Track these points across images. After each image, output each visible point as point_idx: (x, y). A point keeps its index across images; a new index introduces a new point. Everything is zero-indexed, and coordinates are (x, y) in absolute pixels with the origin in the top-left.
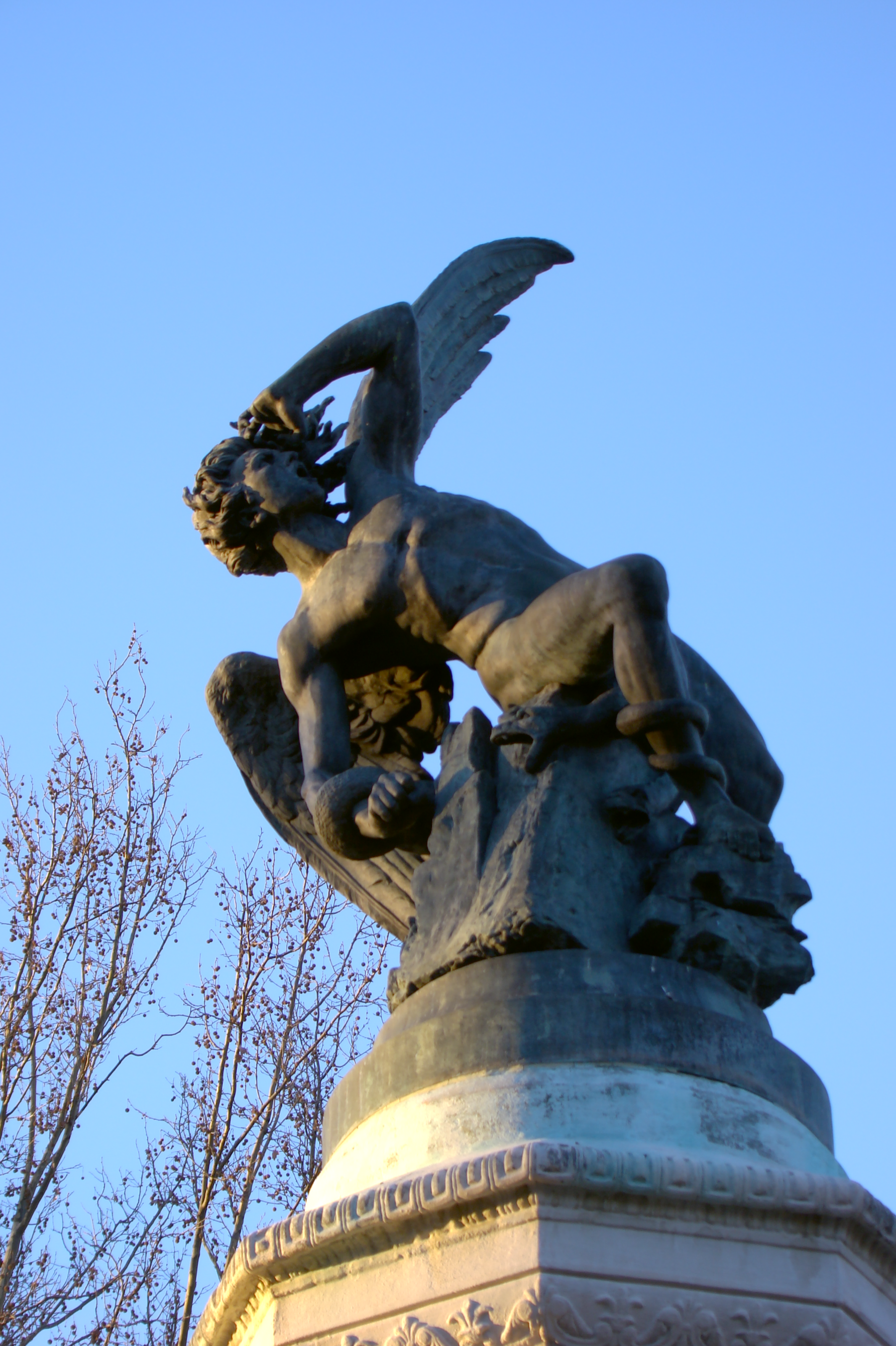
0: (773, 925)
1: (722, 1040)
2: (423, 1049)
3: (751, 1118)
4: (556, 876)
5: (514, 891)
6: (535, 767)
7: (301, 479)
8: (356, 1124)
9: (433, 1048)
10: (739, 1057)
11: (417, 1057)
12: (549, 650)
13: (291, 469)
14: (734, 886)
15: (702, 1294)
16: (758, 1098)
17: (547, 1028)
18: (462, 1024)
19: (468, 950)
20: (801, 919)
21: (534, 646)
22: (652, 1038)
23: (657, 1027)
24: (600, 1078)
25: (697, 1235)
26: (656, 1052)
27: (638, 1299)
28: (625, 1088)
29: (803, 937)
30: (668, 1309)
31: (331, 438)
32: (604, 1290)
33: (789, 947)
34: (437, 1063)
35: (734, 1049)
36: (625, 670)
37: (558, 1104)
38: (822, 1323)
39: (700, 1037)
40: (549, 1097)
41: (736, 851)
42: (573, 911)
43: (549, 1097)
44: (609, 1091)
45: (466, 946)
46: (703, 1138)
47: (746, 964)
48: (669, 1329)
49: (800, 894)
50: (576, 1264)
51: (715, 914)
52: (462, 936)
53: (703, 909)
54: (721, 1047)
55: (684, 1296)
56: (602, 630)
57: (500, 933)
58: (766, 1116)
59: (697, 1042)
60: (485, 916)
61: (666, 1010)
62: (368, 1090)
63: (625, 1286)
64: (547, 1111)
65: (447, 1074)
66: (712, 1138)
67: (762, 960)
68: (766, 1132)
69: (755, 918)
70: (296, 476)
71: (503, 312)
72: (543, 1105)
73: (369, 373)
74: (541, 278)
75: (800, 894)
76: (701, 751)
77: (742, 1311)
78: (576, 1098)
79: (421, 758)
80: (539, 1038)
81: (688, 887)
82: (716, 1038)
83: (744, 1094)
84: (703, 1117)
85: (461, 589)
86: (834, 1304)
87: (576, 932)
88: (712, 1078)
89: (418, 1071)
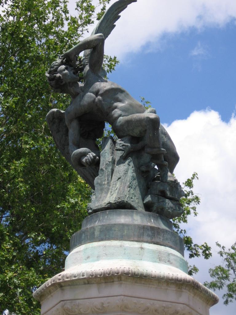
0: (176, 203)
1: (163, 235)
4: (129, 189)
7: (74, 75)
8: (80, 245)
10: (167, 239)
11: (95, 233)
14: (168, 193)
16: (170, 249)
17: (126, 232)
18: (106, 228)
19: (108, 205)
22: (148, 235)
23: (150, 233)
24: (136, 245)
26: (149, 239)
27: (142, 302)
30: (149, 305)
33: (179, 208)
34: (100, 236)
35: (166, 237)
39: (159, 235)
41: (169, 185)
42: (132, 198)
45: (107, 204)
46: (158, 260)
48: (148, 309)
50: (130, 294)
51: (163, 201)
53: (161, 199)
54: (163, 237)
55: (152, 302)
57: (115, 203)
59: (158, 236)
60: (112, 197)
61: (152, 228)
65: (102, 240)
67: (172, 211)
69: (172, 201)
70: (73, 74)
71: (119, 15)
74: (128, 6)
76: (163, 160)
77: (164, 305)
80: (124, 234)
81: (157, 192)
82: (162, 234)
83: (167, 248)
85: (110, 107)
87: (133, 204)
88: (161, 245)
89: (95, 237)
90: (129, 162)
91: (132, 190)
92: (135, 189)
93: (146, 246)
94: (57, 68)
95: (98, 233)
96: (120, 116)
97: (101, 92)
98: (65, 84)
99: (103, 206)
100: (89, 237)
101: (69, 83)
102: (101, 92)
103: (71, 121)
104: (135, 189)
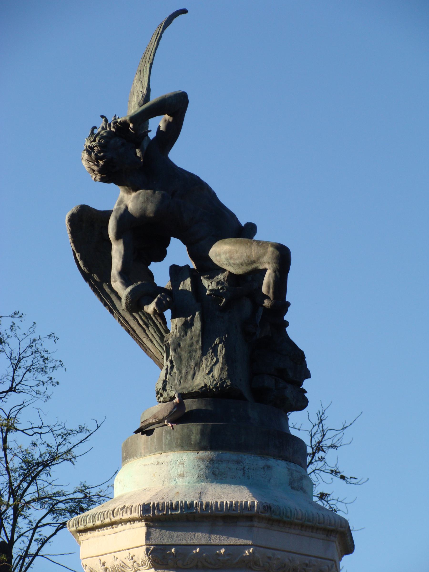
2: (195, 434)
5: (222, 369)
9: (199, 436)
11: (192, 437)
12: (234, 264)
15: (297, 555)
20: (306, 385)
21: (227, 259)
24: (261, 462)
25: (297, 534)
32: (269, 553)
34: (200, 443)
36: (269, 287)
37: (247, 471)
38: (328, 566)
40: (244, 468)
43: (244, 468)
44: (264, 468)
45: (202, 387)
46: (289, 487)
49: (308, 375)
56: (261, 267)
62: (167, 441)
63: (276, 552)
64: (244, 473)
66: (292, 488)
72: (242, 470)
75: (308, 375)
77: (307, 562)
78: (253, 469)
79: (149, 264)
84: (290, 479)
86: (332, 560)
93: (272, 462)
95: (198, 437)
99: (196, 389)
100: (179, 440)
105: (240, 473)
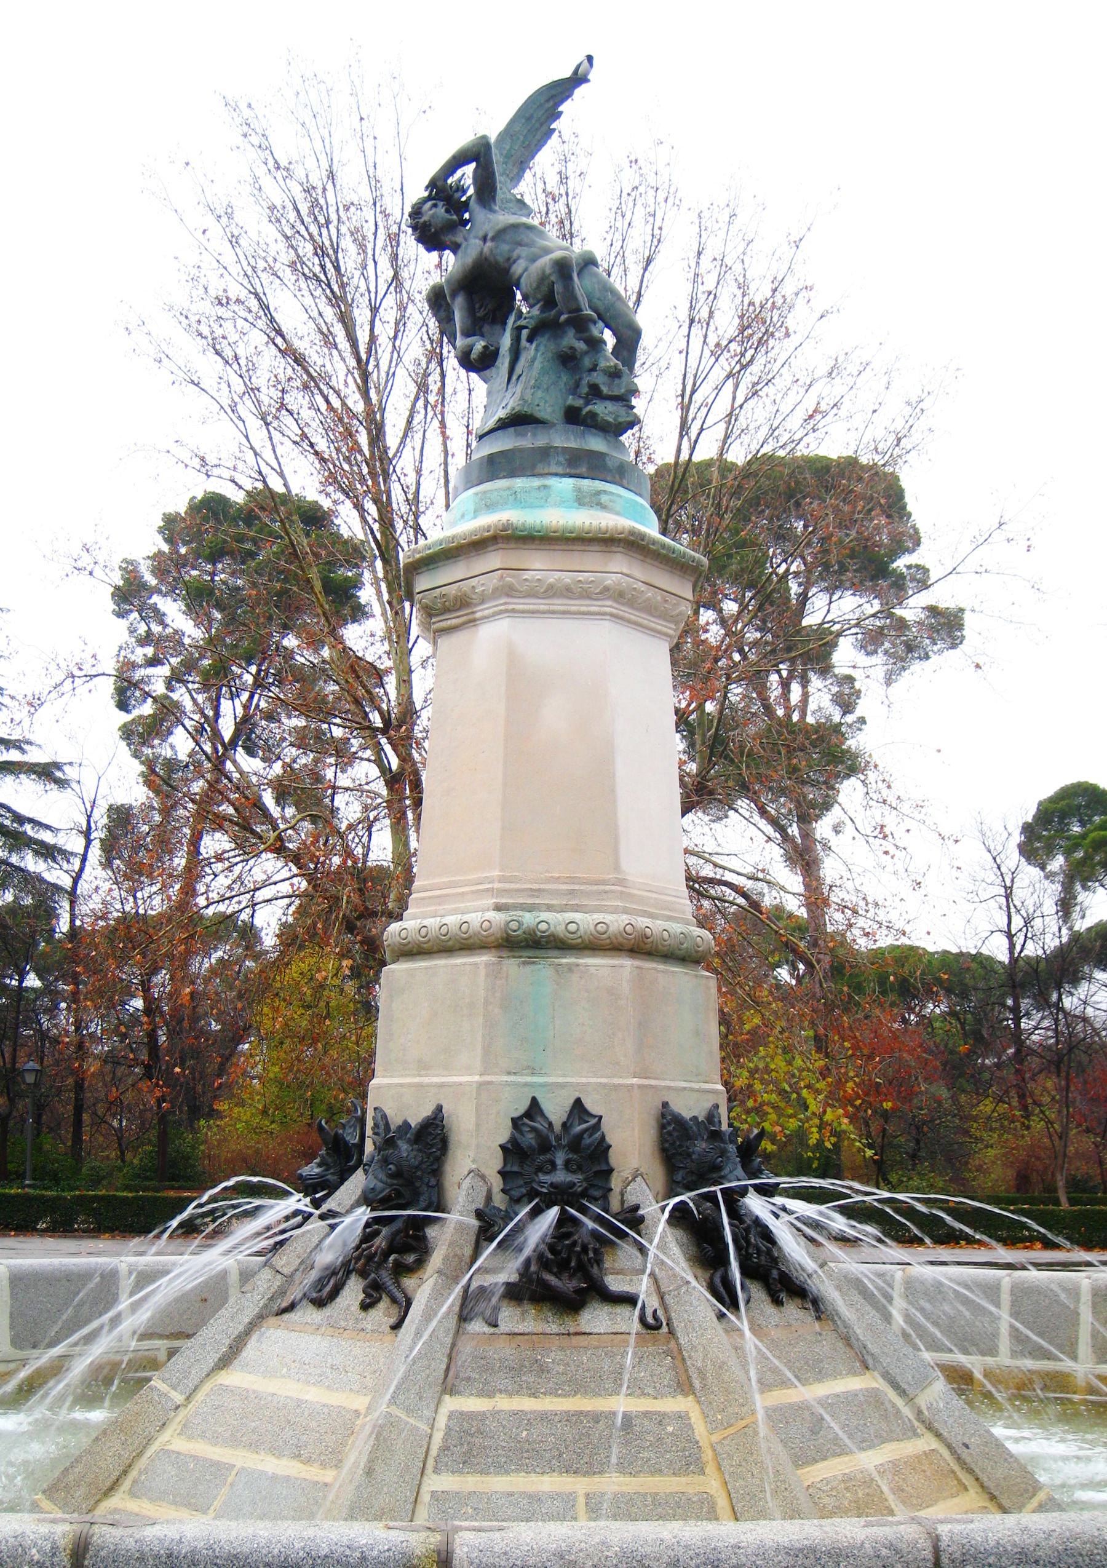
3: (599, 493)
6: (530, 340)
13: (443, 210)
14: (605, 390)
24: (536, 482)
28: (545, 487)
29: (634, 407)
31: (464, 192)
46: (576, 504)
47: (608, 423)
52: (496, 418)
58: (605, 492)
67: (615, 419)
68: (604, 498)
71: (560, 109)
73: (474, 165)
83: (597, 482)
85: (509, 259)
90: (537, 346)
91: (540, 392)
92: (547, 390)
93: (552, 481)
94: (420, 208)
96: (526, 270)
97: (490, 235)
98: (436, 233)
101: (441, 229)
102: (490, 235)
103: (454, 295)
104: (547, 390)
105: (511, 498)
